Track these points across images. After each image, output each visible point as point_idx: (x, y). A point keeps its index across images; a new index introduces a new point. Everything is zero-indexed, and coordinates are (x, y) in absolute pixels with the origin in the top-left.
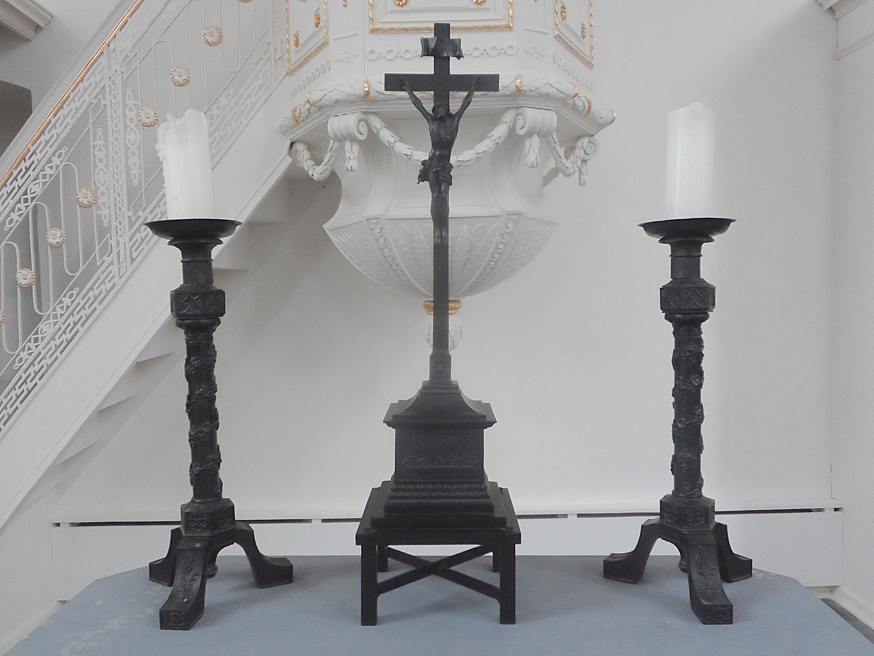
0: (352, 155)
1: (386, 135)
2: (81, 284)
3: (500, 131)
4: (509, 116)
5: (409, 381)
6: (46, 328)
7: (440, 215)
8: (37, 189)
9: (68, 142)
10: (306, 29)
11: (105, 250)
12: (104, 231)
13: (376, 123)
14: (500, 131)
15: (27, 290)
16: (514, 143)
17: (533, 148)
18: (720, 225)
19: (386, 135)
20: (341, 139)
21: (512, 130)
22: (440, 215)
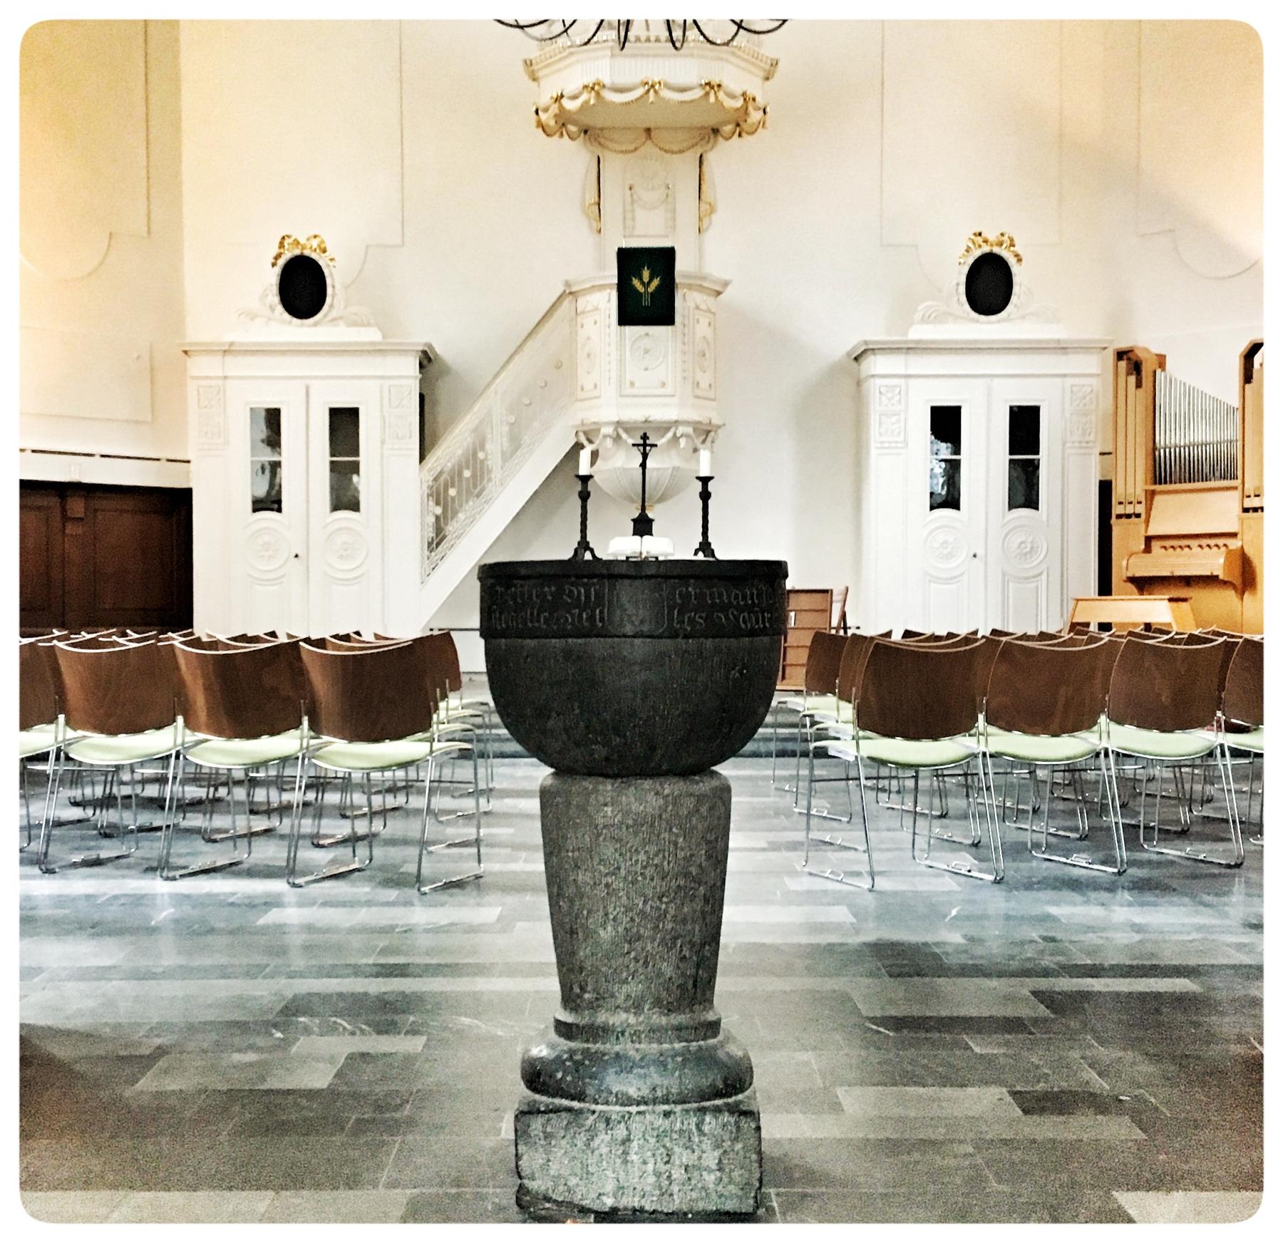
0: (609, 442)
1: (624, 436)
2: (478, 496)
3: (670, 435)
4: (673, 430)
5: (636, 514)
6: (461, 516)
7: (643, 465)
8: (460, 452)
9: (475, 430)
10: (589, 386)
11: (490, 480)
12: (490, 471)
13: (620, 431)
14: (670, 435)
15: (453, 498)
16: (676, 439)
17: (683, 442)
18: (711, 478)
19: (624, 436)
20: (605, 436)
21: (675, 434)
22: (643, 465)
